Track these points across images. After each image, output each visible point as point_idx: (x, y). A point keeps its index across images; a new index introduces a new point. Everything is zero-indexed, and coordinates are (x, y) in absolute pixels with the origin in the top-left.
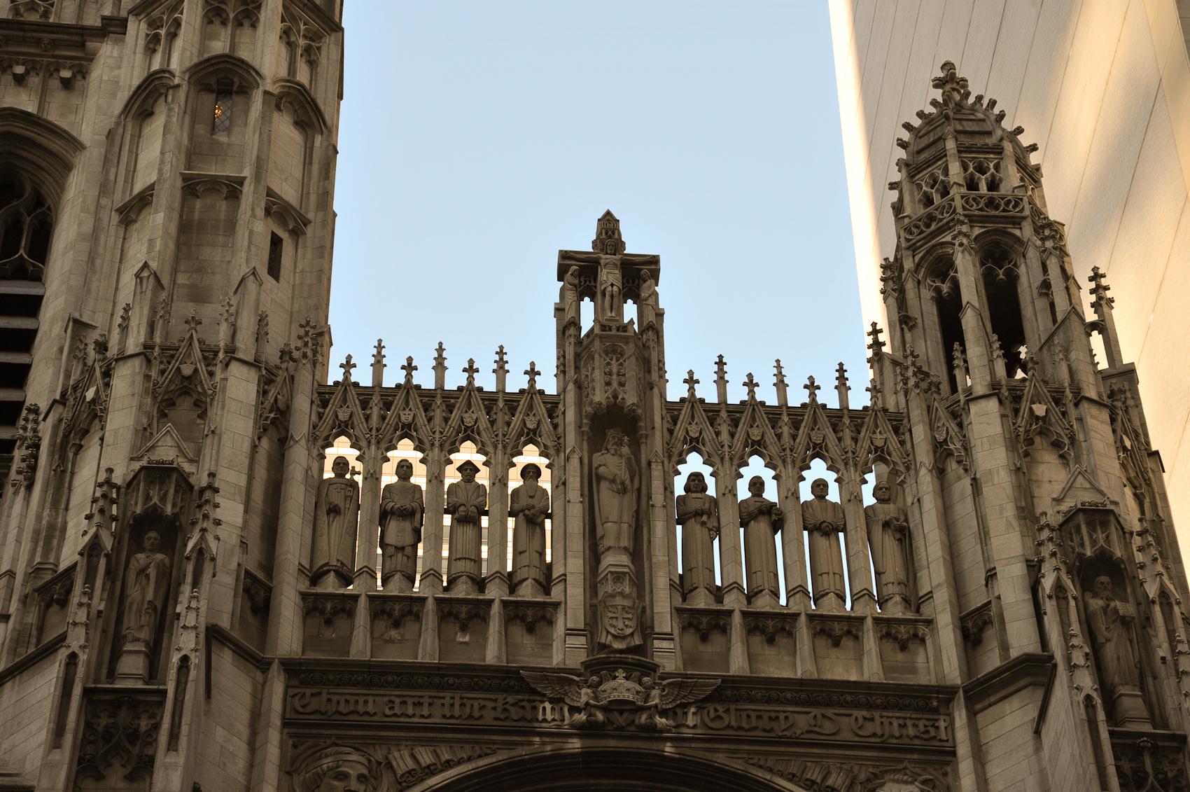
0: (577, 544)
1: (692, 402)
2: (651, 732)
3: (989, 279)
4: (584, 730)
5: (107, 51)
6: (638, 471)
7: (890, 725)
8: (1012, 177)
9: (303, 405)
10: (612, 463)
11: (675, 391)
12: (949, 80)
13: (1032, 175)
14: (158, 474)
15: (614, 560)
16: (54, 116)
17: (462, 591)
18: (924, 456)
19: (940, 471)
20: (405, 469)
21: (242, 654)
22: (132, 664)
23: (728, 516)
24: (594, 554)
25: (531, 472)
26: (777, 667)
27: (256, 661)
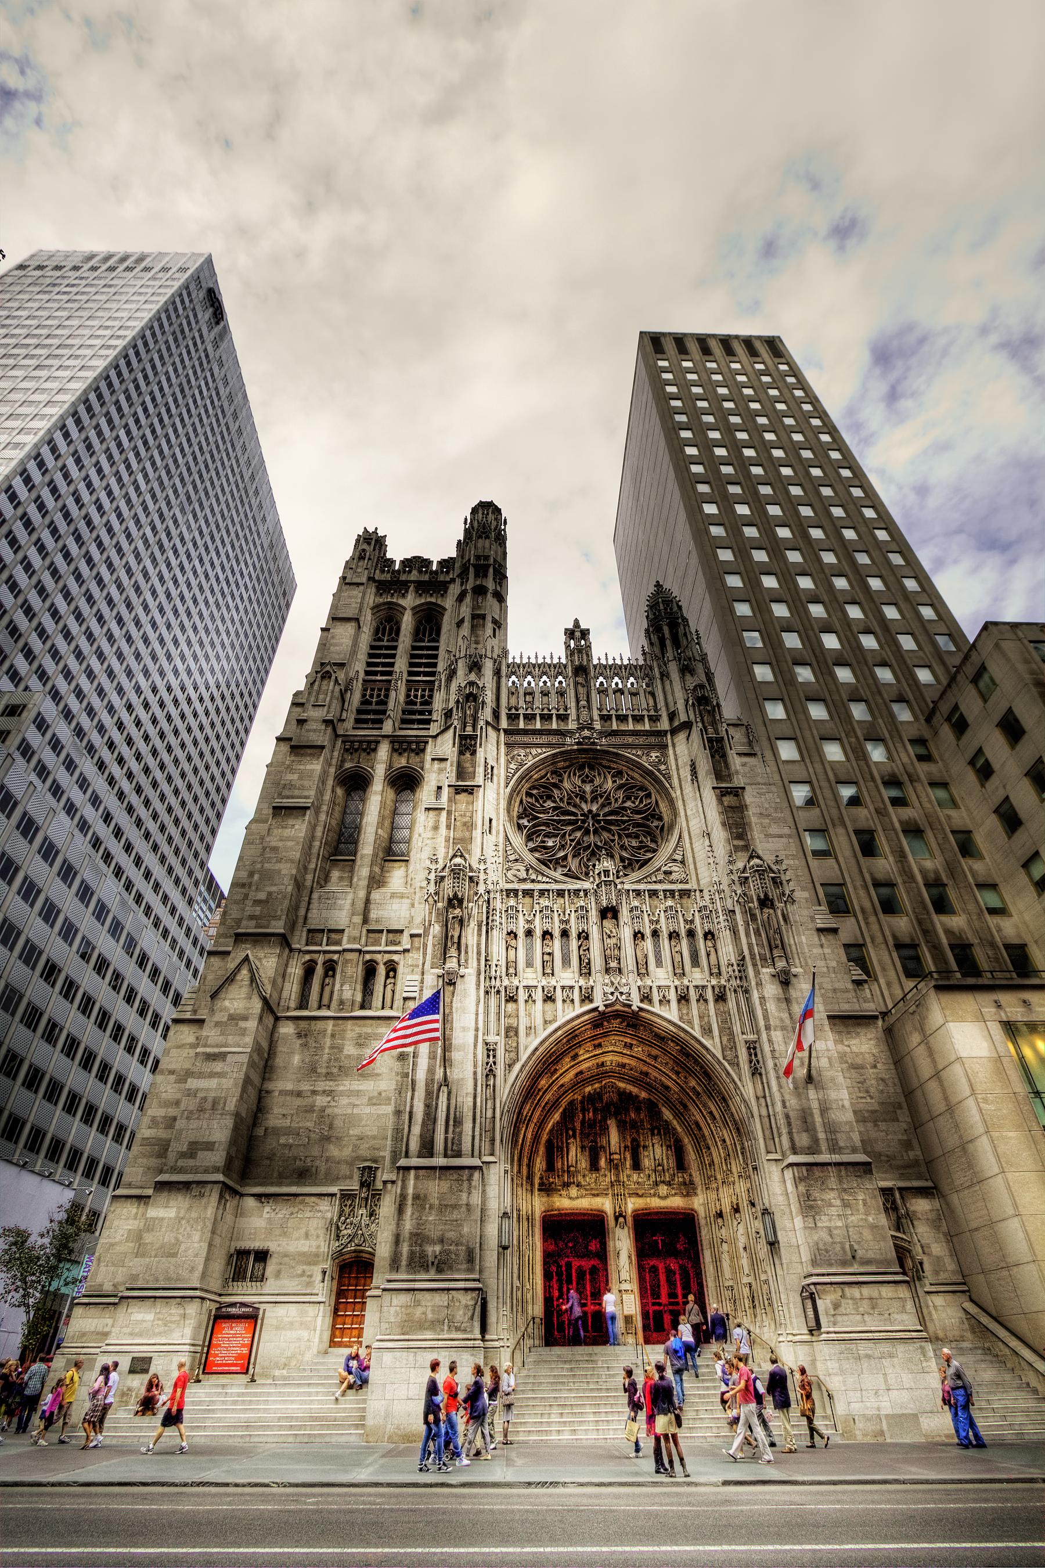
0: (573, 699)
1: (600, 664)
2: (594, 743)
3: (671, 632)
4: (578, 743)
5: (452, 586)
6: (587, 681)
7: (653, 740)
8: (675, 608)
9: (504, 668)
10: (580, 680)
11: (595, 662)
12: (658, 585)
13: (680, 608)
14: (472, 684)
15: (583, 703)
16: (439, 602)
17: (546, 712)
18: (657, 675)
19: (662, 680)
20: (529, 683)
21: (494, 727)
22: (469, 729)
23: (610, 692)
24: (578, 701)
25: (560, 683)
26: (623, 727)
27: (497, 730)
